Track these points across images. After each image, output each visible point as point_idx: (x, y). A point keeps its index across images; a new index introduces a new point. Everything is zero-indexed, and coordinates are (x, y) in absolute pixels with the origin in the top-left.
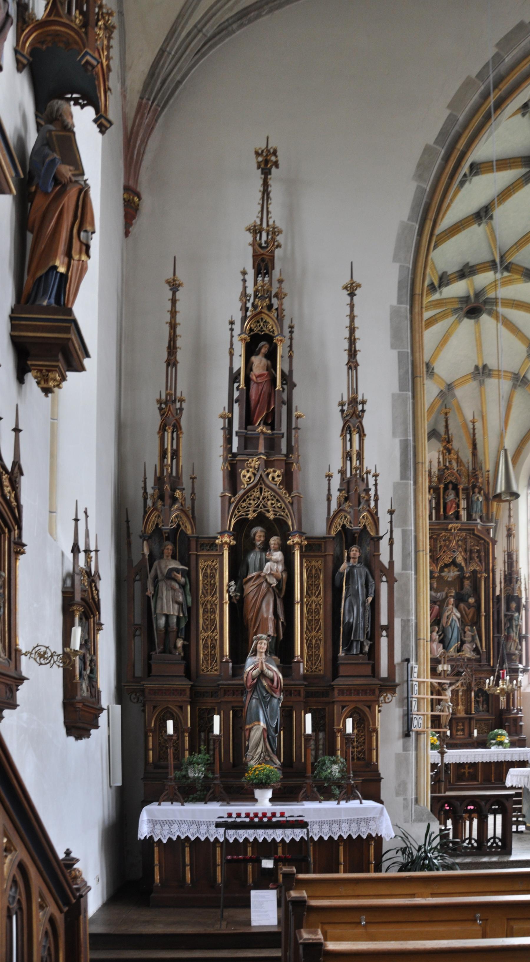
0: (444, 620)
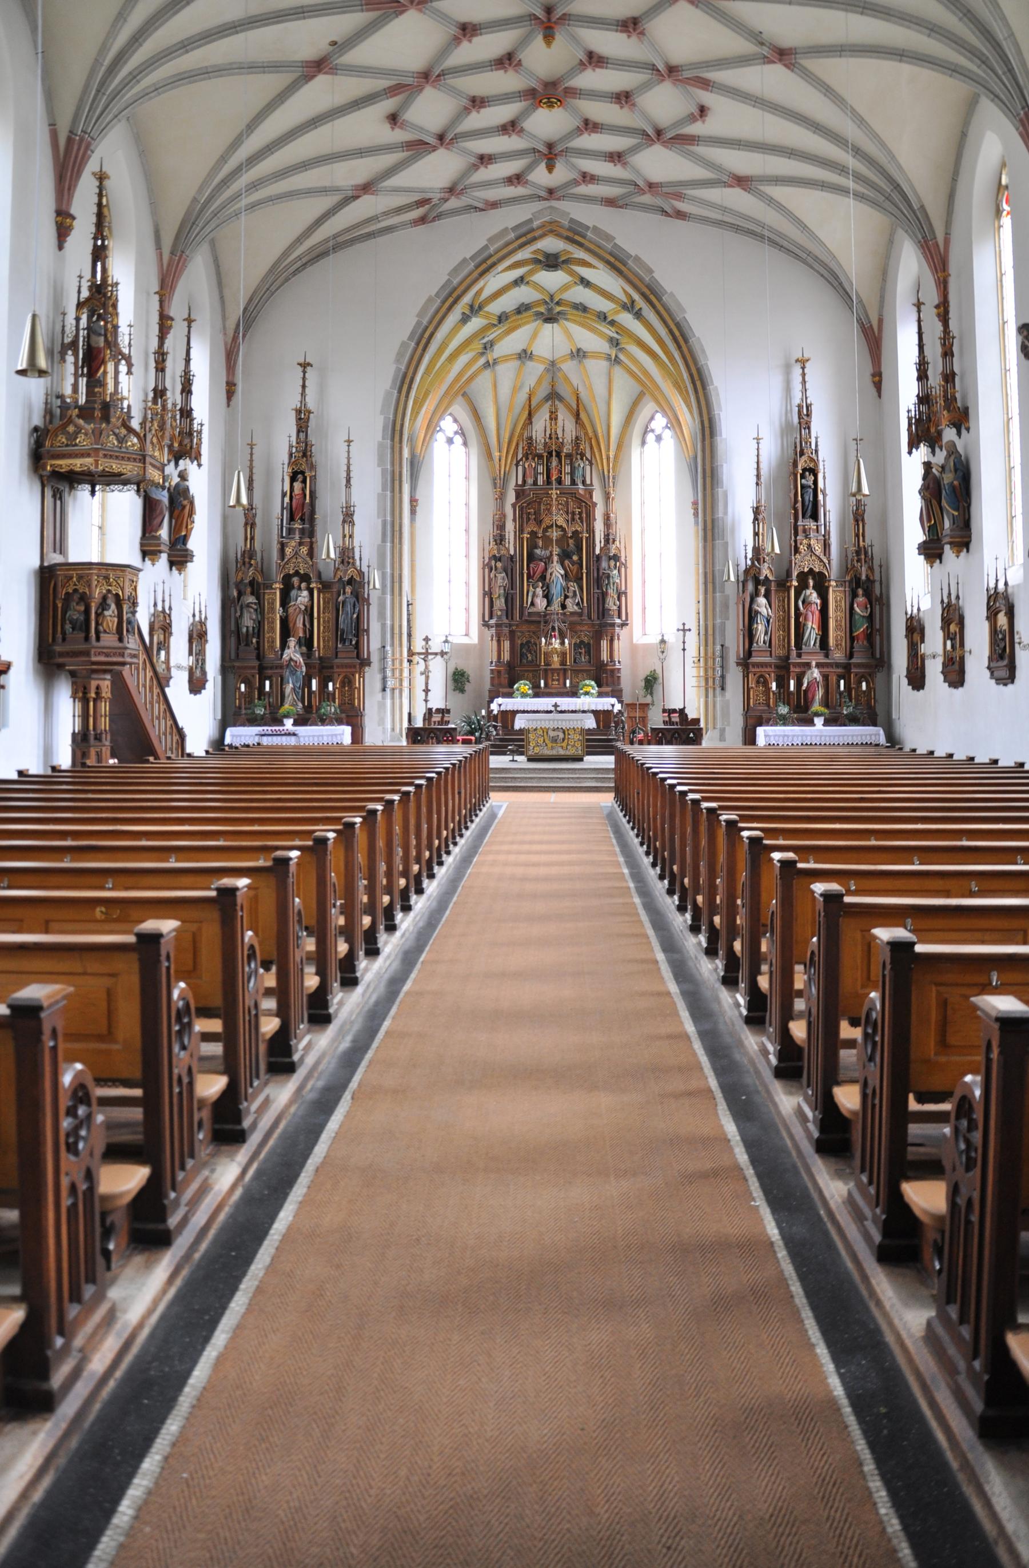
0: (548, 576)
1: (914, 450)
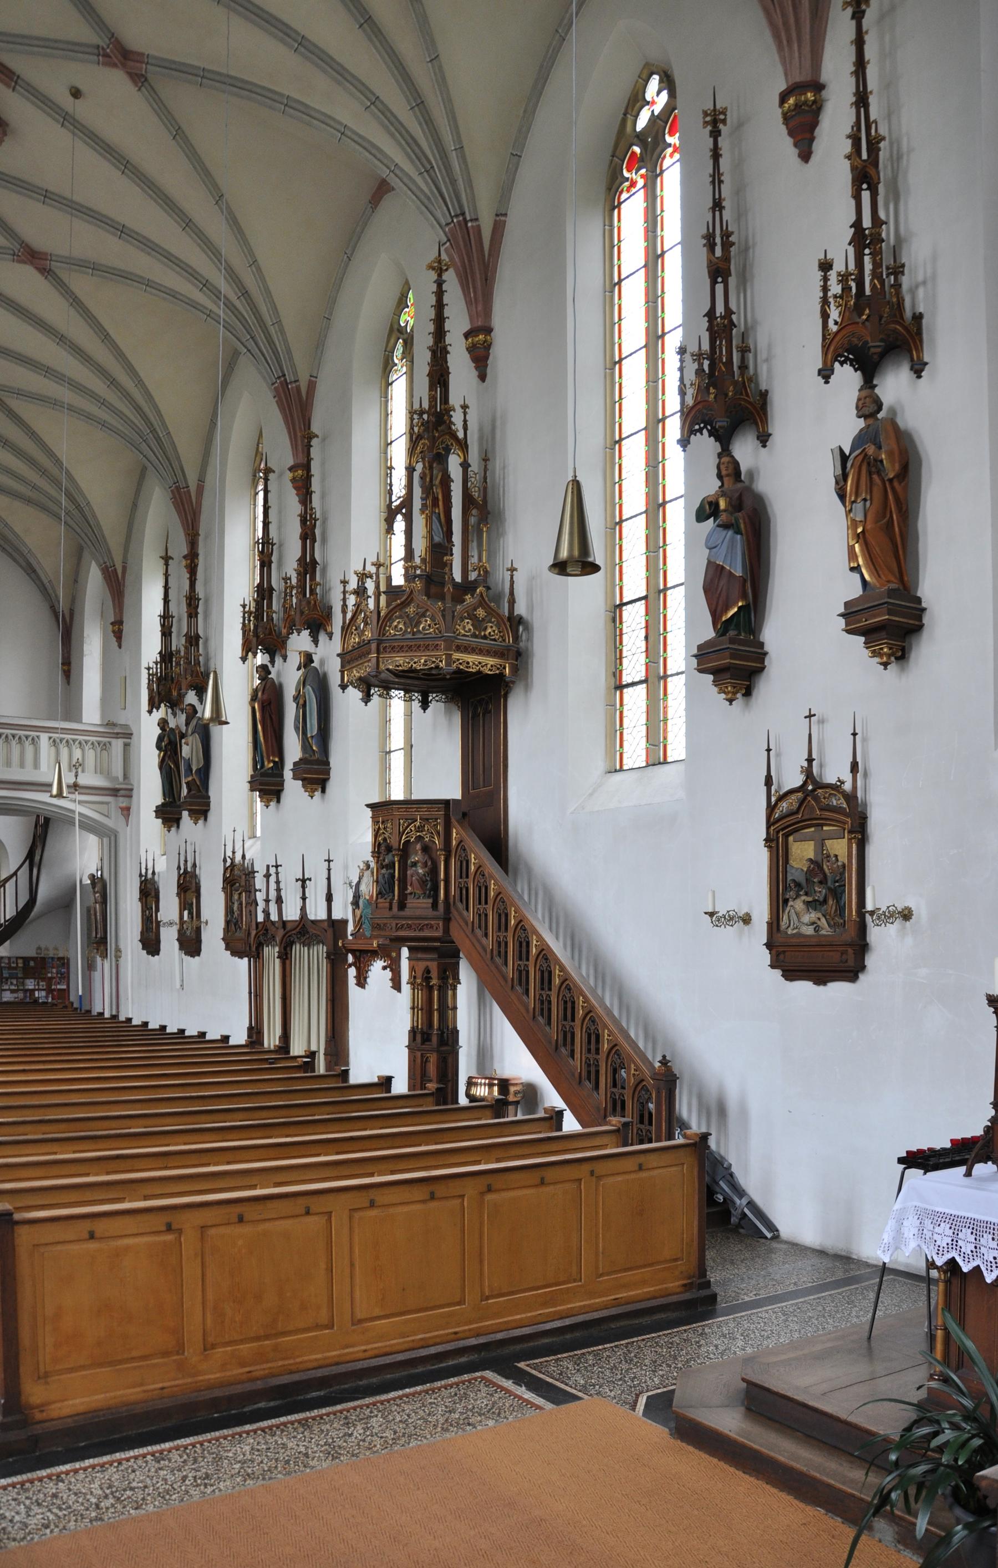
1: (154, 710)
